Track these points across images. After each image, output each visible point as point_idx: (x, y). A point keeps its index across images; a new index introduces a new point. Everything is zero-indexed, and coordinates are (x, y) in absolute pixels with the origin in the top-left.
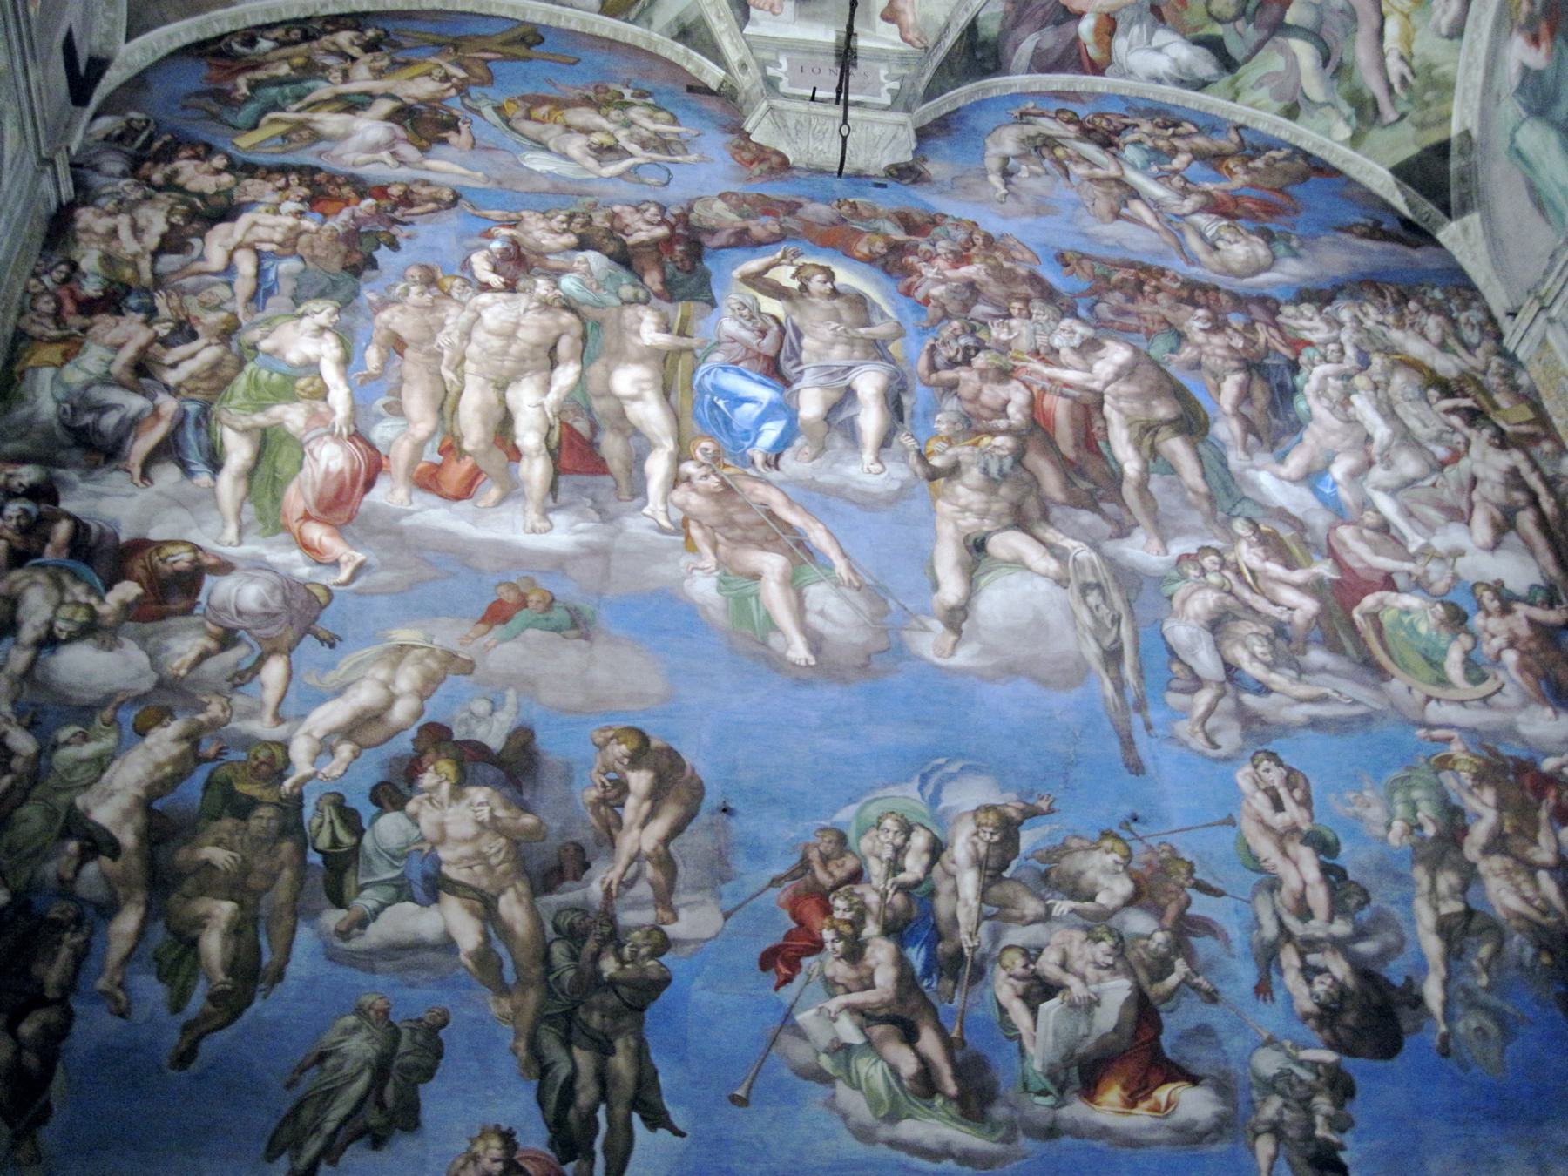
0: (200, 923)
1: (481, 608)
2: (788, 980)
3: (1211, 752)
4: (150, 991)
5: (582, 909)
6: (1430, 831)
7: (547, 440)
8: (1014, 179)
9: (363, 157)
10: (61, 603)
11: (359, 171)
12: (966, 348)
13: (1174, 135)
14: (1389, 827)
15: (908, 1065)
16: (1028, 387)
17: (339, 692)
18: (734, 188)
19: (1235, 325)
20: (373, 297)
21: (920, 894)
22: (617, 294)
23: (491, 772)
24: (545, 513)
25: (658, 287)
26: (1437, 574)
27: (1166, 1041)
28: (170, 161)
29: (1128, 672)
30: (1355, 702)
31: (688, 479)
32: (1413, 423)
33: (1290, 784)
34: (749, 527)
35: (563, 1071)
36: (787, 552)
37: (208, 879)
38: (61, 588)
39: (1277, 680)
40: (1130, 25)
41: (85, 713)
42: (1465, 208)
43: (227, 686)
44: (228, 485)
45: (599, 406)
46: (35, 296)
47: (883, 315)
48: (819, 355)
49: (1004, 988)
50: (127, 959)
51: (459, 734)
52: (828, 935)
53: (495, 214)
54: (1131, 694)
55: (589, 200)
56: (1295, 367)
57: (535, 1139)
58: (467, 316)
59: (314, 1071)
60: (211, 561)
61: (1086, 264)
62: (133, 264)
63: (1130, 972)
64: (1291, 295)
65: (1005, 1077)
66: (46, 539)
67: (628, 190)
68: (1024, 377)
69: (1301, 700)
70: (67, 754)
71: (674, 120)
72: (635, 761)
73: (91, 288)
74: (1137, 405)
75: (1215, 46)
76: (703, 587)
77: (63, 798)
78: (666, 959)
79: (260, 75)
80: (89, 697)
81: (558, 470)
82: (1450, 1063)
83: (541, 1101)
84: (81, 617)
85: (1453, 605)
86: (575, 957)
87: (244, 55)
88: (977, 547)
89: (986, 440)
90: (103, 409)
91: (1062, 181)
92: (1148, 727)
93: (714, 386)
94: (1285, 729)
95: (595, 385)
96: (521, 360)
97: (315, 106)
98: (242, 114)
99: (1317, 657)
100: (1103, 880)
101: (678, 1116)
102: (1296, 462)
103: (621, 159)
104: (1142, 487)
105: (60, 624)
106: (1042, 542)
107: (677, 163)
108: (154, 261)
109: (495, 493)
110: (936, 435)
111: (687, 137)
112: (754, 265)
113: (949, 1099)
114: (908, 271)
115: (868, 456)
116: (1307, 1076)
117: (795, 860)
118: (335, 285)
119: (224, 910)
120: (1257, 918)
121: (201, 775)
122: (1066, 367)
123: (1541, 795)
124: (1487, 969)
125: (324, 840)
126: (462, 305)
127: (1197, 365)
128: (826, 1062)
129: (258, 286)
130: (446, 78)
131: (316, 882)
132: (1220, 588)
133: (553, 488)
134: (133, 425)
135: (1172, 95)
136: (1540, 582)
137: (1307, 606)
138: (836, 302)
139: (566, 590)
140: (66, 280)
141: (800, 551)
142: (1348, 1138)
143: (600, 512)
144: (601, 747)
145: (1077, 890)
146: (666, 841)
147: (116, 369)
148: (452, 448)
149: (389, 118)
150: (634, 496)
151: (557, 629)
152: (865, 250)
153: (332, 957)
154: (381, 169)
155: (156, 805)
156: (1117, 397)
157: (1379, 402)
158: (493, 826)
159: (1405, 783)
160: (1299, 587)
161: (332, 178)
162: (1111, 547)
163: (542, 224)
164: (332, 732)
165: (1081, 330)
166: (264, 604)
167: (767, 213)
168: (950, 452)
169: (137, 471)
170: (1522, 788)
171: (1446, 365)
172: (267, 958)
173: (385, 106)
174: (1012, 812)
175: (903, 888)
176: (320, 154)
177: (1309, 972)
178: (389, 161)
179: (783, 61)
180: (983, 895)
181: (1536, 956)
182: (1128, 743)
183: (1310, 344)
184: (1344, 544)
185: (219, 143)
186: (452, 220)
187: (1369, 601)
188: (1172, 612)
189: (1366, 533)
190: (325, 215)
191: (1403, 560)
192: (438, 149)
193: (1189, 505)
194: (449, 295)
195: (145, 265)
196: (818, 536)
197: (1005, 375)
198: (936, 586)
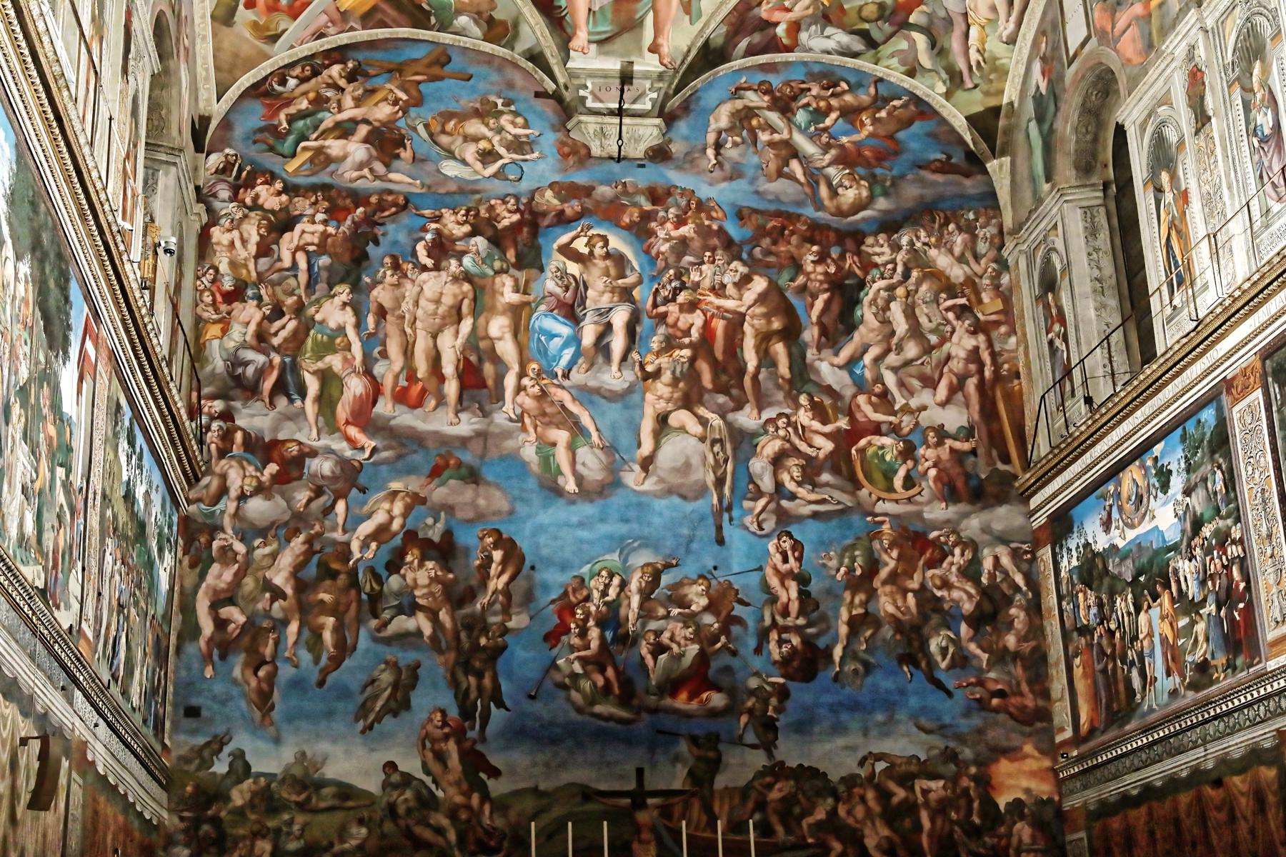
0: (322, 627)
1: (427, 470)
2: (555, 646)
3: (759, 532)
4: (305, 657)
5: (472, 616)
6: (858, 572)
7: (457, 368)
8: (722, 151)
9: (355, 174)
10: (245, 476)
11: (354, 185)
12: (675, 289)
13: (833, 95)
14: (838, 570)
15: (600, 681)
16: (705, 315)
17: (369, 516)
18: (557, 178)
19: (834, 255)
20: (367, 280)
21: (614, 606)
22: (492, 267)
23: (433, 553)
24: (456, 414)
25: (513, 260)
26: (907, 422)
27: (711, 673)
28: (253, 188)
29: (727, 491)
30: (839, 503)
31: (525, 389)
32: (923, 320)
33: (794, 549)
34: (553, 415)
35: (464, 686)
36: (570, 430)
37: (323, 608)
38: (243, 468)
39: (802, 492)
40: (810, 25)
41: (263, 532)
42: (1003, 154)
43: (321, 516)
44: (310, 407)
45: (483, 344)
46: (202, 292)
47: (633, 269)
48: (595, 302)
49: (644, 650)
50: (295, 643)
51: (421, 535)
52: (573, 626)
53: (427, 212)
54: (725, 503)
55: (477, 196)
56: (862, 285)
57: (454, 713)
58: (417, 289)
59: (369, 689)
60: (307, 450)
61: (754, 217)
62: (246, 266)
63: (700, 642)
64: (874, 227)
65: (640, 685)
66: (233, 443)
67: (500, 187)
68: (704, 307)
69: (810, 502)
70: (259, 553)
71: (526, 126)
72: (496, 546)
73: (228, 284)
74: (763, 322)
75: (865, 35)
76: (529, 453)
77: (260, 574)
78: (507, 638)
79: (292, 110)
80: (265, 524)
81: (463, 388)
82: (837, 686)
83: (456, 696)
84: (254, 483)
85: (910, 442)
86: (469, 637)
87: (281, 93)
88: (662, 420)
89: (677, 352)
90: (246, 364)
91: (752, 149)
92: (731, 519)
93: (540, 328)
94: (800, 519)
95: (481, 333)
96: (443, 318)
97: (324, 135)
98: (286, 145)
99: (826, 477)
100: (696, 599)
101: (508, 703)
102: (846, 353)
103: (495, 161)
104: (755, 377)
105: (246, 488)
106: (696, 415)
107: (526, 160)
108: (256, 264)
109: (433, 403)
110: (649, 351)
111: (532, 137)
112: (564, 239)
113: (615, 696)
114: (652, 233)
115: (615, 367)
116: (768, 688)
117: (561, 591)
118: (348, 273)
119: (330, 621)
120: (763, 617)
121: (316, 559)
122: (726, 297)
123: (922, 554)
124: (867, 641)
125: (368, 588)
126: (413, 281)
127: (803, 289)
128: (567, 681)
129: (310, 276)
130: (396, 102)
131: (366, 607)
132: (784, 439)
133: (460, 399)
134: (261, 373)
135: (838, 60)
136: (966, 425)
137: (828, 446)
138: (608, 262)
139: (467, 457)
140: (213, 281)
141: (577, 429)
142: (781, 717)
143: (481, 409)
144: (482, 539)
145: (683, 603)
146: (508, 584)
147: (248, 338)
148: (412, 377)
149: (366, 140)
150: (498, 401)
151: (462, 478)
152: (626, 219)
153: (376, 640)
154: (367, 184)
155: (299, 575)
156: (752, 317)
157: (907, 305)
158: (435, 580)
159: (853, 547)
160: (826, 435)
161: (339, 190)
162: (730, 416)
163: (453, 218)
164: (367, 537)
165: (743, 269)
166: (333, 472)
167: (575, 197)
168: (657, 362)
169: (267, 400)
170: (914, 547)
171: (957, 273)
172: (349, 641)
173: (363, 130)
174: (659, 566)
175: (606, 604)
176: (332, 173)
177: (781, 642)
178: (369, 176)
179: (589, 84)
180: (641, 607)
181: (894, 636)
182: (719, 528)
183: (876, 266)
184: (859, 406)
185: (277, 170)
186: (405, 219)
187: (863, 442)
188: (754, 454)
189: (873, 398)
190: (340, 222)
191: (890, 415)
192: (396, 164)
193: (779, 387)
194: (405, 276)
195: (251, 265)
196: (586, 420)
197: (692, 306)
198: (639, 445)
